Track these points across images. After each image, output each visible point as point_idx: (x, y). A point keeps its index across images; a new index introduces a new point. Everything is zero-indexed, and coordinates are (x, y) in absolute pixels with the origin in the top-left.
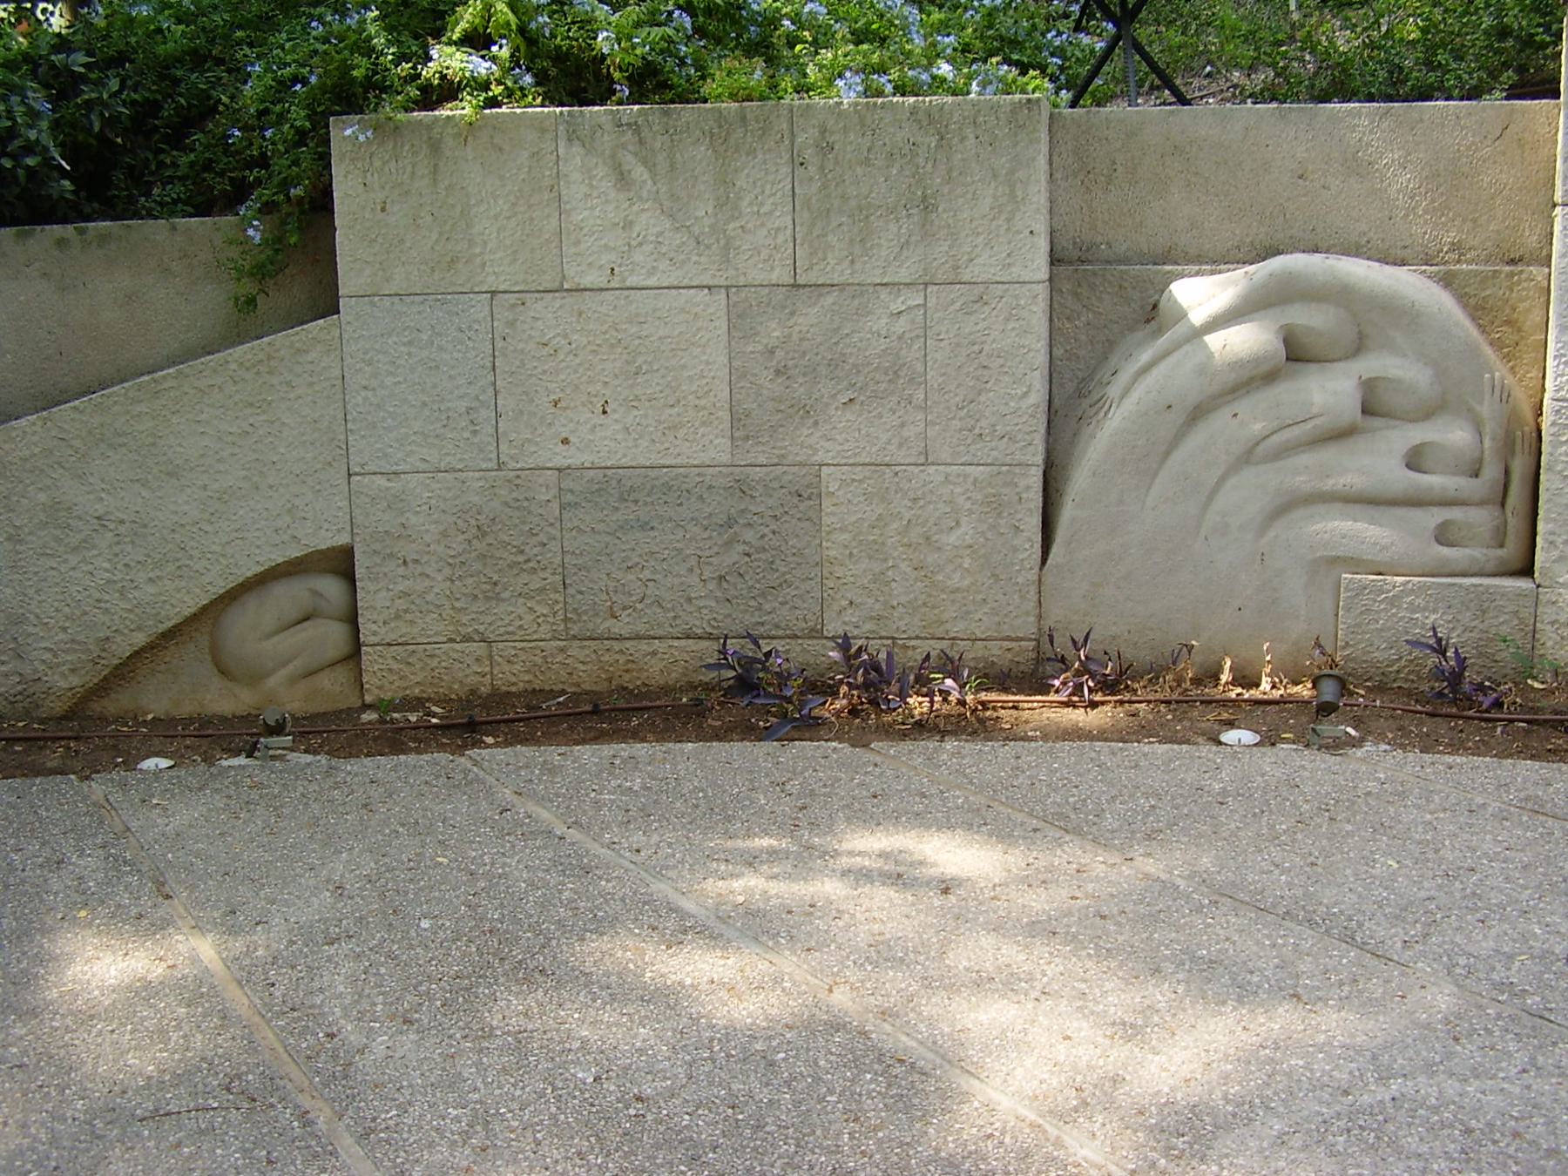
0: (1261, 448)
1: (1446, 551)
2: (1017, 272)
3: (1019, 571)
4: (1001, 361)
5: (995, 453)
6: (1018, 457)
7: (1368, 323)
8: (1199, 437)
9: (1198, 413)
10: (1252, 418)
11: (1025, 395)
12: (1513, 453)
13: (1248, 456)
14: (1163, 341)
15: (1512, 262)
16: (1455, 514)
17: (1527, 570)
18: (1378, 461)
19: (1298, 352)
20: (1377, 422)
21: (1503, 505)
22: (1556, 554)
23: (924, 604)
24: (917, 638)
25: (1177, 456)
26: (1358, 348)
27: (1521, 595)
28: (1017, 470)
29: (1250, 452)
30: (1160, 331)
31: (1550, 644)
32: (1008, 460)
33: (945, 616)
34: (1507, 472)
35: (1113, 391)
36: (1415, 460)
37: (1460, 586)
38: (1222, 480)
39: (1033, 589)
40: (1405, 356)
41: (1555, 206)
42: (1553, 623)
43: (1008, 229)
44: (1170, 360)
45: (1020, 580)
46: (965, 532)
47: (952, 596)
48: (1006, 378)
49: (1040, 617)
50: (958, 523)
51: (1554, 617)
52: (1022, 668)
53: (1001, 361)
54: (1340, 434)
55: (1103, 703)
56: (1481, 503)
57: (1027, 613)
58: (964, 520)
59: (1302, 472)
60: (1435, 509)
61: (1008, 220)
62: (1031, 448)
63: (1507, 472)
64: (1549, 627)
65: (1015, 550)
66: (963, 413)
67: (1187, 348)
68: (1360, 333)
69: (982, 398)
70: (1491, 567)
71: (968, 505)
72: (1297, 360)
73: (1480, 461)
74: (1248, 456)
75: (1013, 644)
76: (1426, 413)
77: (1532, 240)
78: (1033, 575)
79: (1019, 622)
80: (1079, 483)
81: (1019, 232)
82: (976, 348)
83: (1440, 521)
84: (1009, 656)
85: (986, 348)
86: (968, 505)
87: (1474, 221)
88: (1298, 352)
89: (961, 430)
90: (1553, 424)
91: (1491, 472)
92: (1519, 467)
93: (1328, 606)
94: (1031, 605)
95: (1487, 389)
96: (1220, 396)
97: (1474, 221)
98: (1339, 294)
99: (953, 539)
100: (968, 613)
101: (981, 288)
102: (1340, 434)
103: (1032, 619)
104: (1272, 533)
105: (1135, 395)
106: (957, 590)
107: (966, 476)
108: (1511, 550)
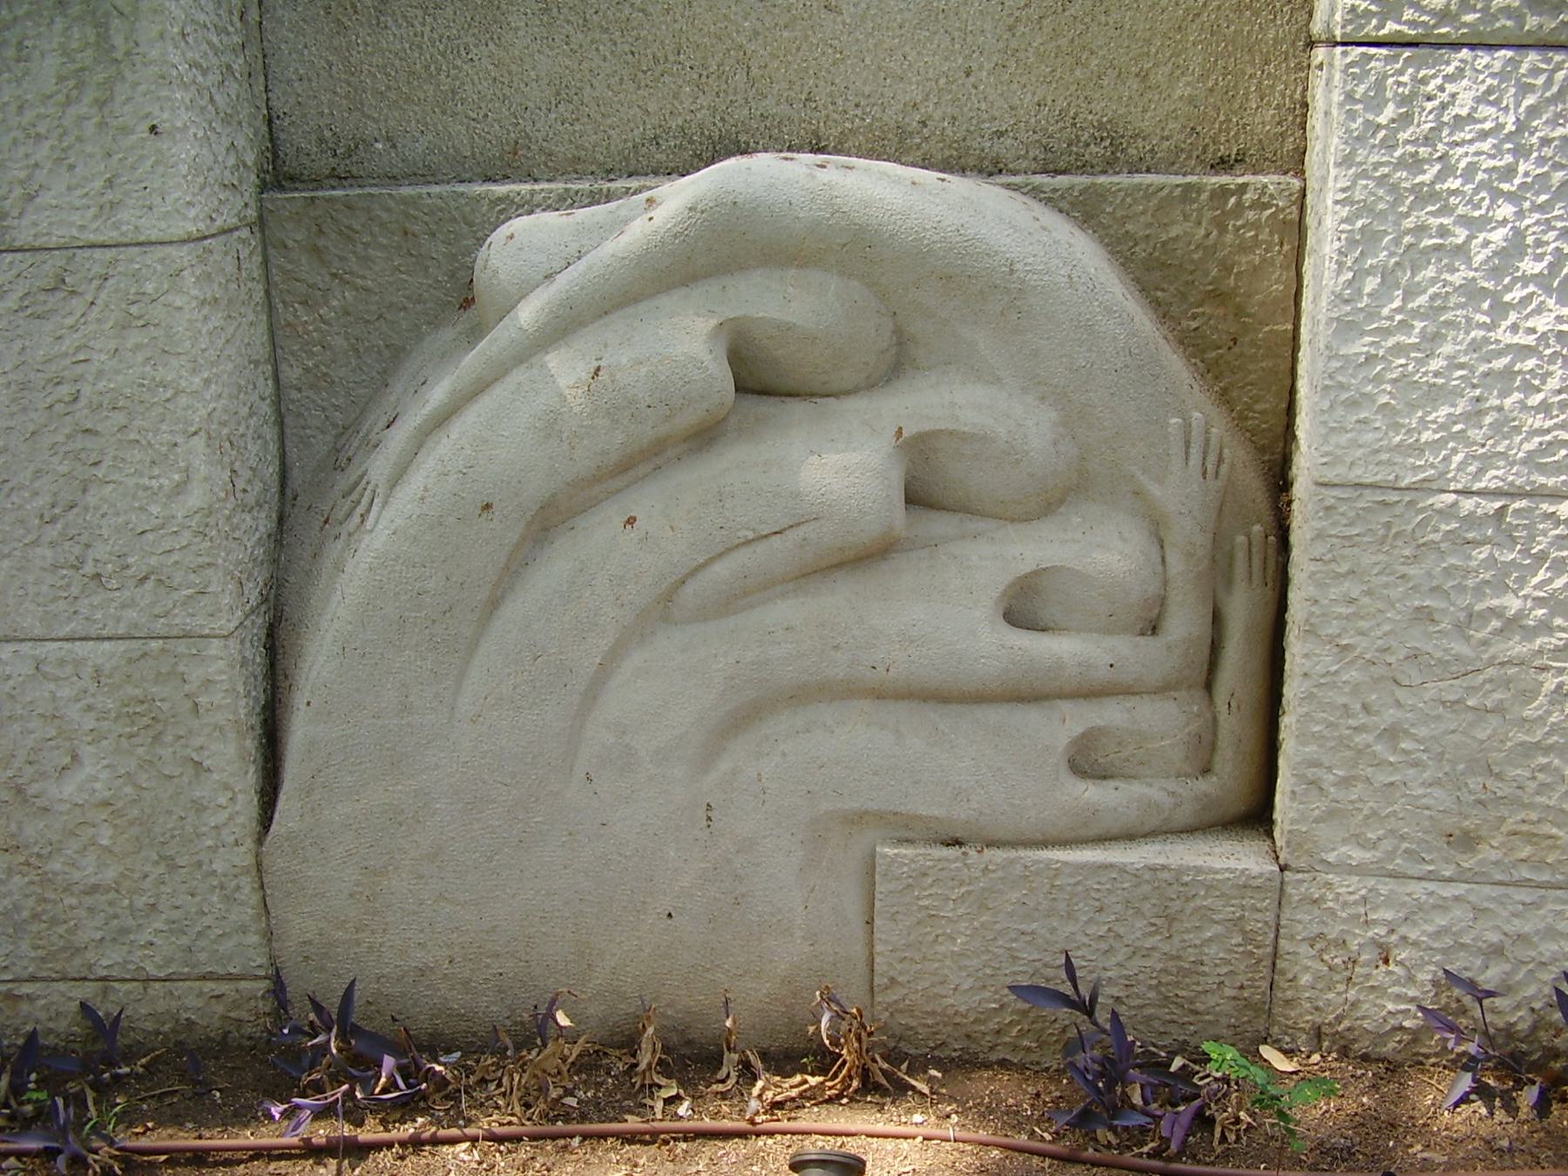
0: (689, 589)
1: (1091, 793)
2: (130, 221)
3: (213, 849)
4: (120, 418)
5: (132, 614)
6: (180, 619)
7: (911, 310)
8: (553, 571)
9: (549, 520)
10: (665, 520)
11: (180, 489)
12: (1229, 582)
13: (665, 607)
14: (472, 361)
15: (1223, 164)
16: (1111, 714)
17: (1255, 816)
18: (946, 611)
19: (761, 379)
20: (941, 524)
21: (1208, 686)
22: (1318, 806)
23: (36, 917)
24: (33, 979)
25: (513, 611)
26: (897, 363)
27: (1246, 886)
28: (182, 647)
29: (669, 597)
30: (476, 333)
31: (1305, 979)
32: (159, 626)
33: (83, 937)
34: (1217, 619)
35: (378, 467)
36: (1022, 608)
37: (1122, 869)
38: (614, 655)
39: (247, 884)
40: (997, 381)
41: (1311, 44)
42: (1312, 942)
43: (102, 125)
44: (487, 402)
45: (218, 866)
46: (92, 776)
47: (89, 901)
48: (137, 455)
49: (269, 935)
50: (75, 757)
51: (1315, 929)
52: (248, 1030)
53: (120, 418)
54: (866, 557)
55: (377, 1146)
56: (1164, 689)
57: (244, 930)
58: (87, 751)
59: (792, 630)
60: (1066, 706)
61: (101, 104)
62: (205, 600)
63: (1217, 619)
64: (1304, 949)
65: (200, 808)
66: (53, 532)
67: (518, 376)
68: (898, 332)
69: (91, 499)
70: (1185, 815)
71: (90, 722)
72: (765, 392)
73: (1163, 601)
74: (665, 607)
75: (224, 987)
76: (1047, 502)
77: (1263, 121)
78: (243, 856)
79: (227, 946)
80: (318, 666)
81: (125, 130)
82: (65, 391)
83: (1080, 730)
84: (219, 1009)
85: (87, 390)
86: (90, 722)
87: (1143, 76)
88: (761, 379)
89: (55, 567)
90: (1320, 536)
91: (1184, 624)
92: (1243, 610)
93: (853, 908)
94: (246, 912)
95: (1176, 449)
96: (596, 479)
97: (1143, 76)
98: (848, 248)
99: (69, 789)
100: (125, 931)
101: (59, 259)
102: (866, 557)
103: (254, 939)
104: (724, 765)
105: (417, 481)
106: (94, 889)
107: (79, 663)
108: (1228, 780)
